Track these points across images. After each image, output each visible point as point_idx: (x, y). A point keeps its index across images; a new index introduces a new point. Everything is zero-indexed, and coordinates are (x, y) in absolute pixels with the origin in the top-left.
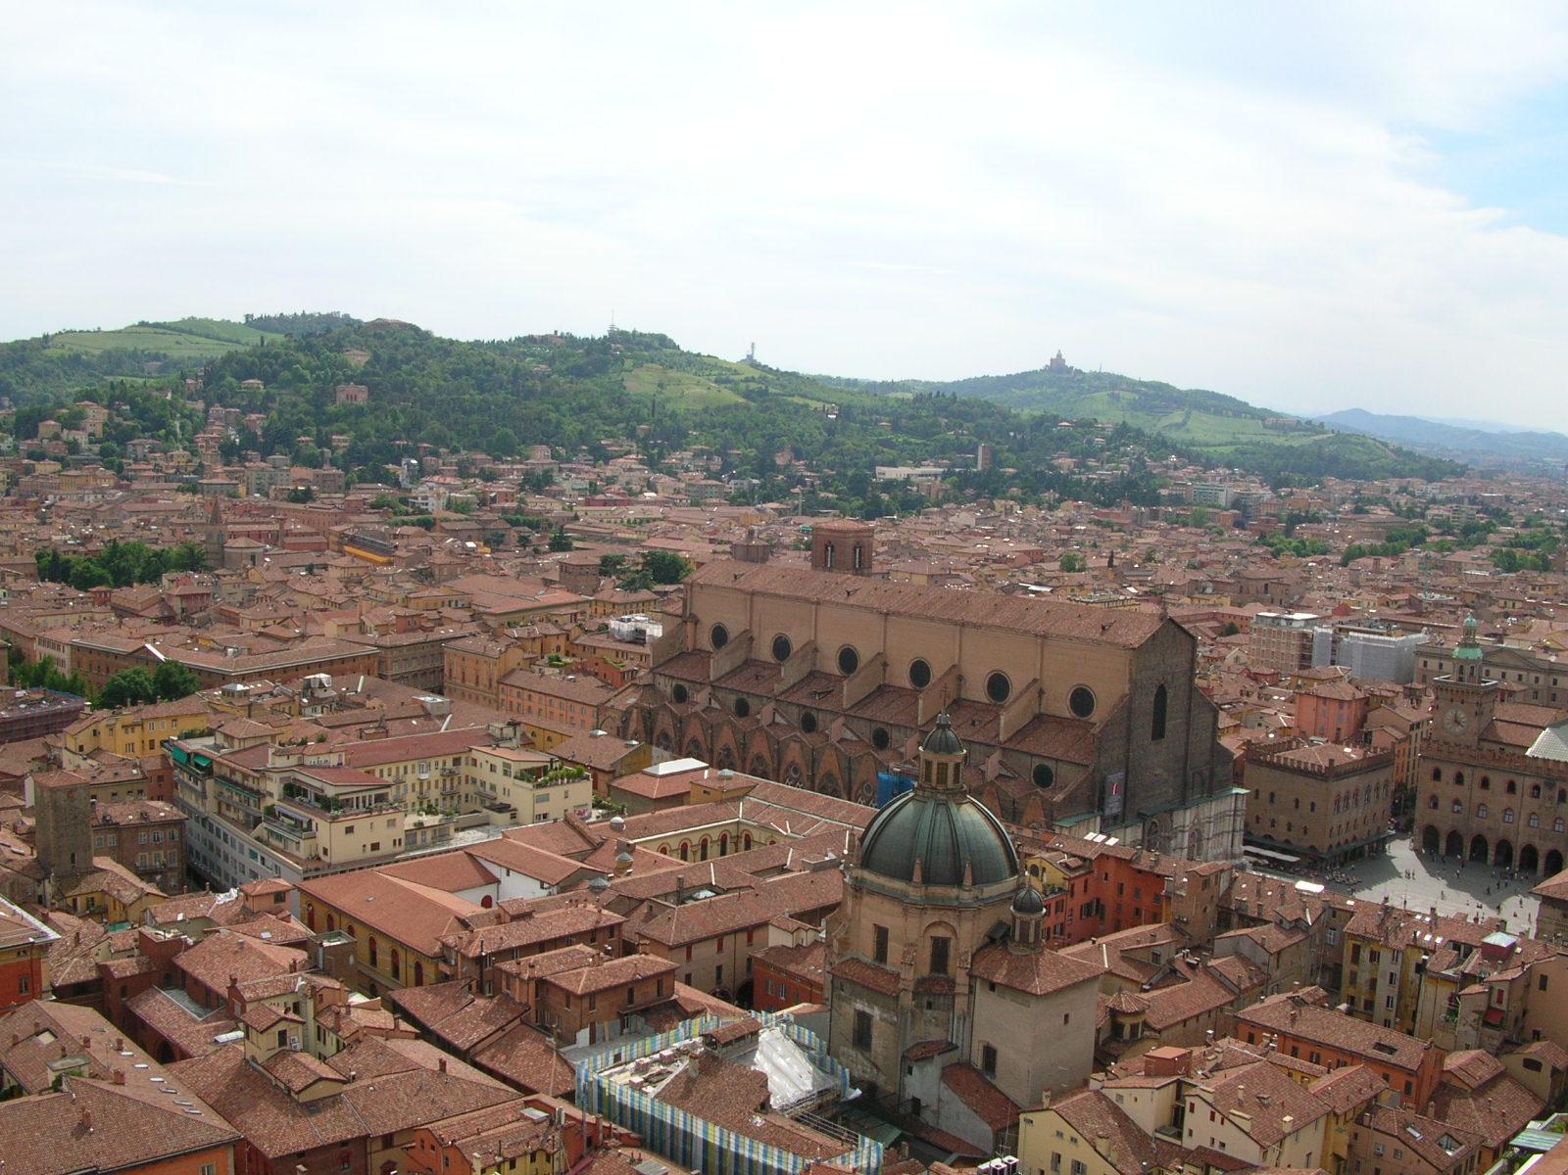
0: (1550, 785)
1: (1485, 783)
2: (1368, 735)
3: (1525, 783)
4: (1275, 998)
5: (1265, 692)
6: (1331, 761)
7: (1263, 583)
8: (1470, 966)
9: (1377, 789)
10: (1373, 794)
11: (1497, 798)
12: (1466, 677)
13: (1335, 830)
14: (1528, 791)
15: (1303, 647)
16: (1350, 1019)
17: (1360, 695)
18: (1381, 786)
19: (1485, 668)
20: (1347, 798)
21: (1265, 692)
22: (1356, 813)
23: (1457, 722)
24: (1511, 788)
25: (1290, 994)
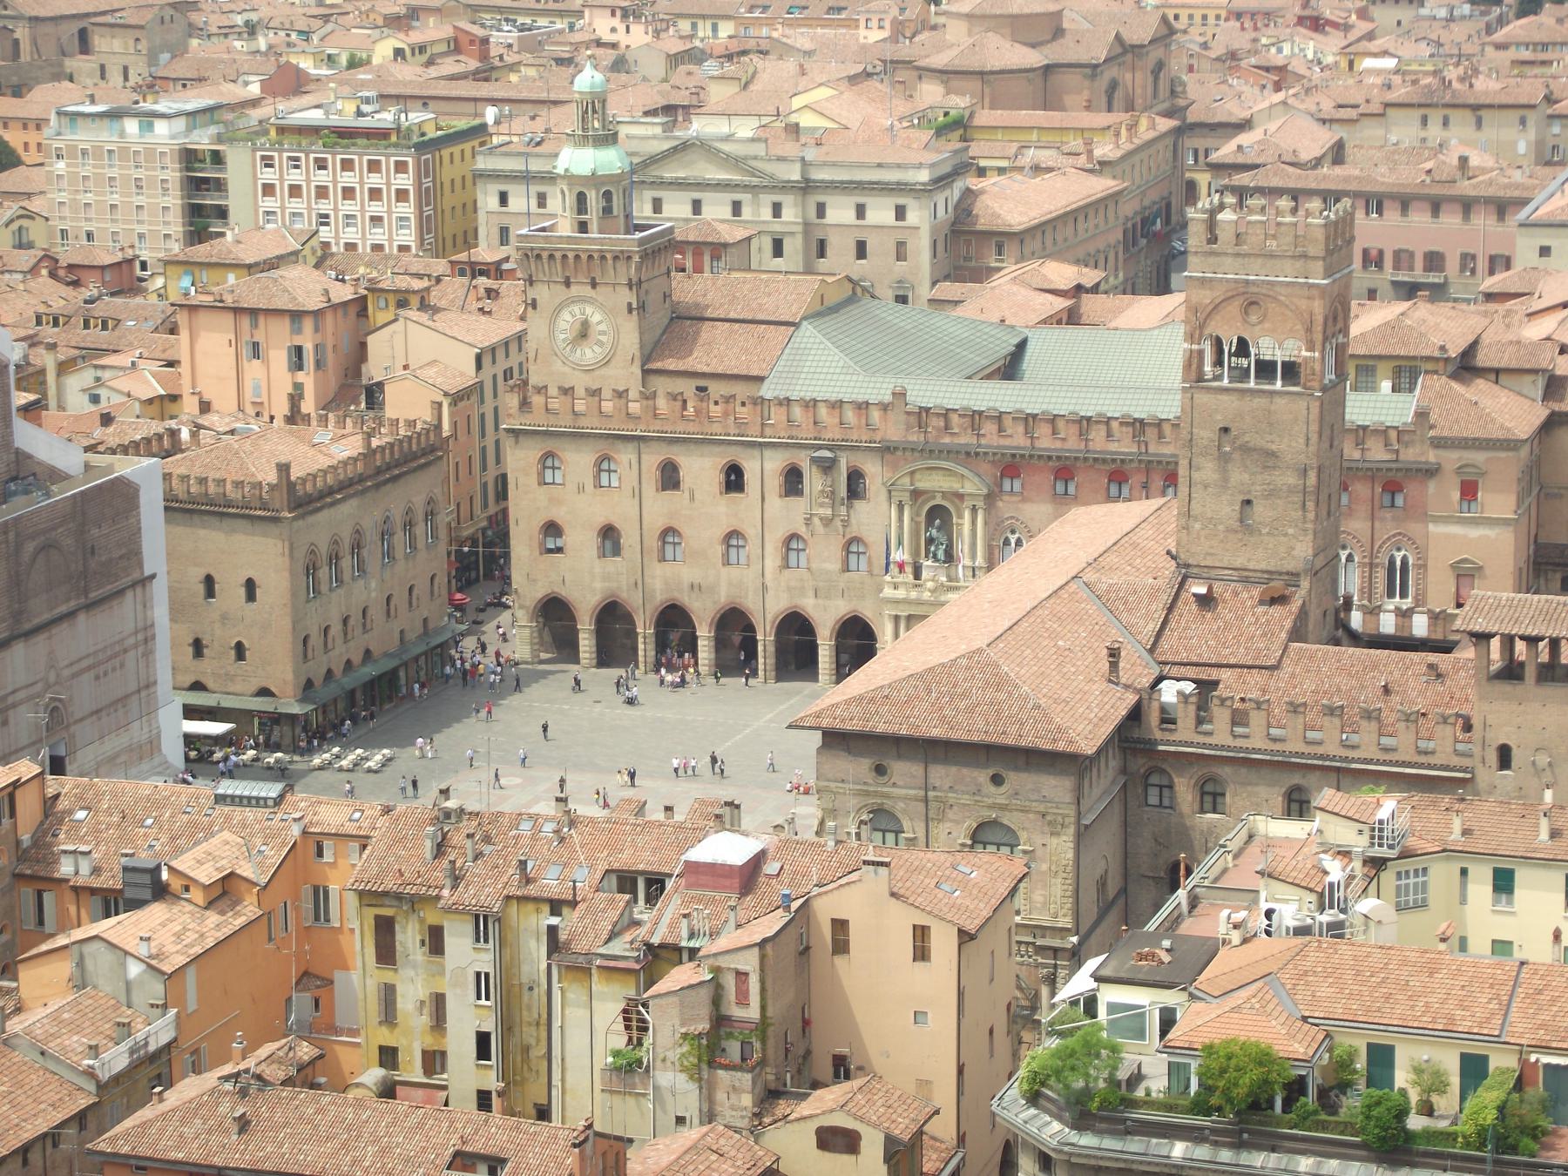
0: (827, 466)
1: (670, 477)
2: (374, 395)
3: (763, 469)
4: (188, 1089)
5: (99, 310)
6: (284, 469)
7: (75, 27)
8: (662, 922)
9: (409, 525)
10: (399, 539)
11: (703, 506)
12: (593, 216)
13: (316, 641)
14: (774, 483)
15: (196, 185)
16: (384, 1105)
17: (343, 293)
18: (420, 516)
19: (649, 195)
20: (334, 559)
21: (99, 310)
22: (366, 591)
23: (584, 332)
24: (734, 479)
25: (228, 1069)
